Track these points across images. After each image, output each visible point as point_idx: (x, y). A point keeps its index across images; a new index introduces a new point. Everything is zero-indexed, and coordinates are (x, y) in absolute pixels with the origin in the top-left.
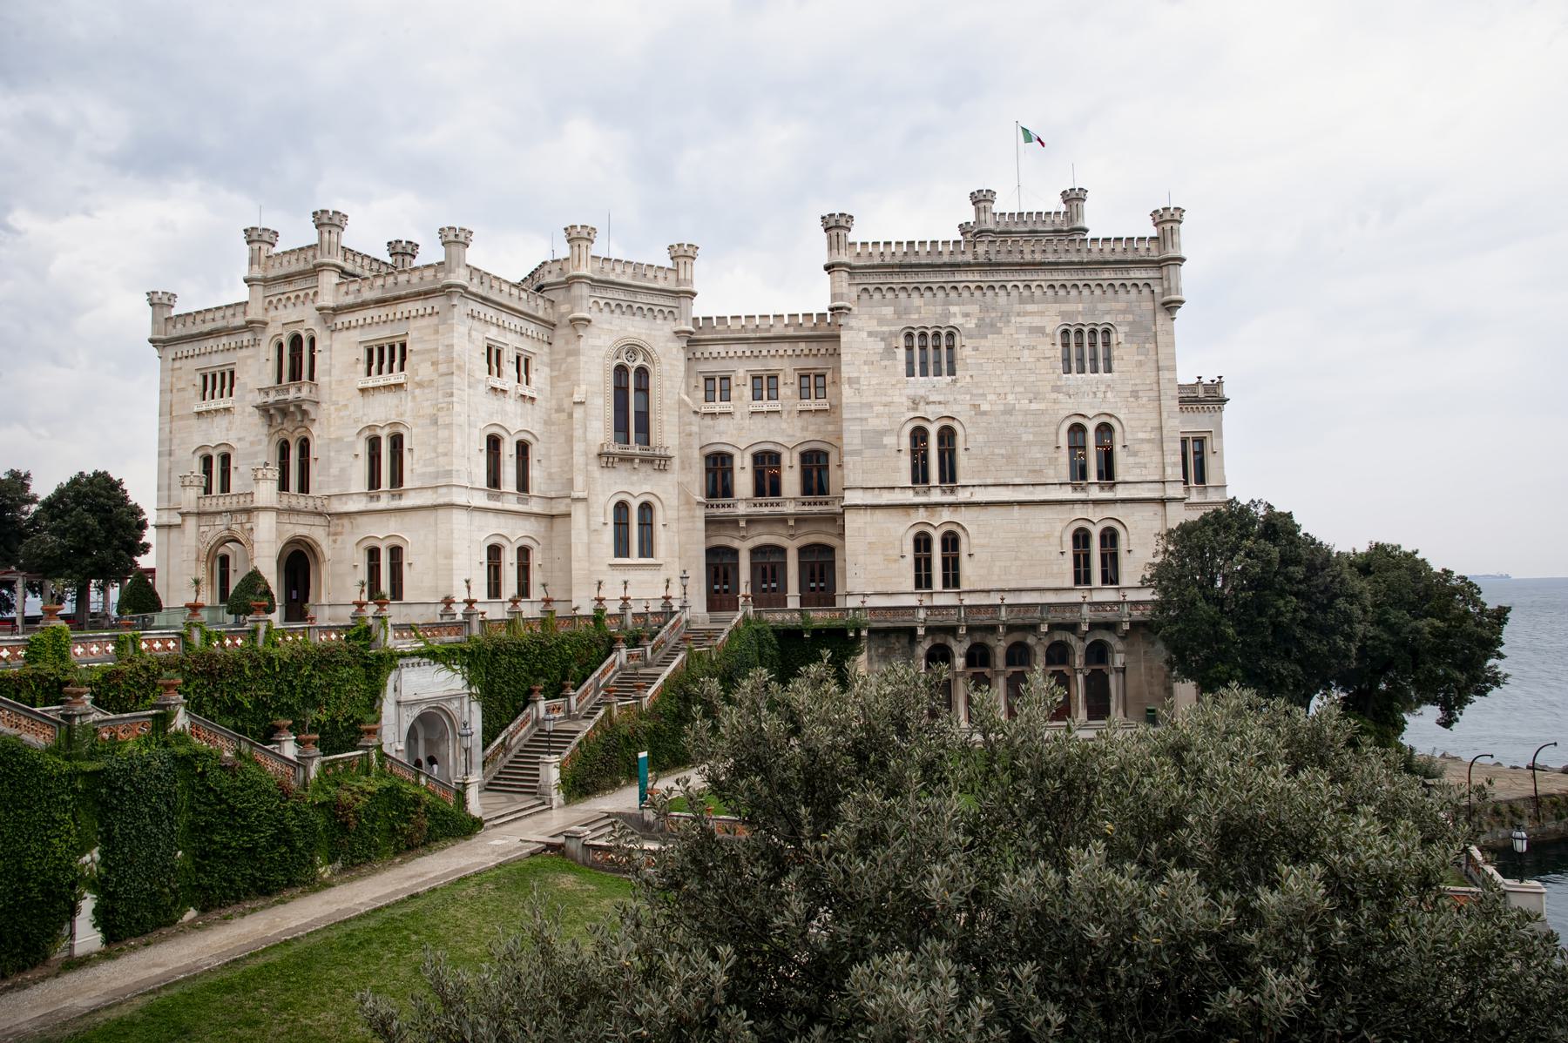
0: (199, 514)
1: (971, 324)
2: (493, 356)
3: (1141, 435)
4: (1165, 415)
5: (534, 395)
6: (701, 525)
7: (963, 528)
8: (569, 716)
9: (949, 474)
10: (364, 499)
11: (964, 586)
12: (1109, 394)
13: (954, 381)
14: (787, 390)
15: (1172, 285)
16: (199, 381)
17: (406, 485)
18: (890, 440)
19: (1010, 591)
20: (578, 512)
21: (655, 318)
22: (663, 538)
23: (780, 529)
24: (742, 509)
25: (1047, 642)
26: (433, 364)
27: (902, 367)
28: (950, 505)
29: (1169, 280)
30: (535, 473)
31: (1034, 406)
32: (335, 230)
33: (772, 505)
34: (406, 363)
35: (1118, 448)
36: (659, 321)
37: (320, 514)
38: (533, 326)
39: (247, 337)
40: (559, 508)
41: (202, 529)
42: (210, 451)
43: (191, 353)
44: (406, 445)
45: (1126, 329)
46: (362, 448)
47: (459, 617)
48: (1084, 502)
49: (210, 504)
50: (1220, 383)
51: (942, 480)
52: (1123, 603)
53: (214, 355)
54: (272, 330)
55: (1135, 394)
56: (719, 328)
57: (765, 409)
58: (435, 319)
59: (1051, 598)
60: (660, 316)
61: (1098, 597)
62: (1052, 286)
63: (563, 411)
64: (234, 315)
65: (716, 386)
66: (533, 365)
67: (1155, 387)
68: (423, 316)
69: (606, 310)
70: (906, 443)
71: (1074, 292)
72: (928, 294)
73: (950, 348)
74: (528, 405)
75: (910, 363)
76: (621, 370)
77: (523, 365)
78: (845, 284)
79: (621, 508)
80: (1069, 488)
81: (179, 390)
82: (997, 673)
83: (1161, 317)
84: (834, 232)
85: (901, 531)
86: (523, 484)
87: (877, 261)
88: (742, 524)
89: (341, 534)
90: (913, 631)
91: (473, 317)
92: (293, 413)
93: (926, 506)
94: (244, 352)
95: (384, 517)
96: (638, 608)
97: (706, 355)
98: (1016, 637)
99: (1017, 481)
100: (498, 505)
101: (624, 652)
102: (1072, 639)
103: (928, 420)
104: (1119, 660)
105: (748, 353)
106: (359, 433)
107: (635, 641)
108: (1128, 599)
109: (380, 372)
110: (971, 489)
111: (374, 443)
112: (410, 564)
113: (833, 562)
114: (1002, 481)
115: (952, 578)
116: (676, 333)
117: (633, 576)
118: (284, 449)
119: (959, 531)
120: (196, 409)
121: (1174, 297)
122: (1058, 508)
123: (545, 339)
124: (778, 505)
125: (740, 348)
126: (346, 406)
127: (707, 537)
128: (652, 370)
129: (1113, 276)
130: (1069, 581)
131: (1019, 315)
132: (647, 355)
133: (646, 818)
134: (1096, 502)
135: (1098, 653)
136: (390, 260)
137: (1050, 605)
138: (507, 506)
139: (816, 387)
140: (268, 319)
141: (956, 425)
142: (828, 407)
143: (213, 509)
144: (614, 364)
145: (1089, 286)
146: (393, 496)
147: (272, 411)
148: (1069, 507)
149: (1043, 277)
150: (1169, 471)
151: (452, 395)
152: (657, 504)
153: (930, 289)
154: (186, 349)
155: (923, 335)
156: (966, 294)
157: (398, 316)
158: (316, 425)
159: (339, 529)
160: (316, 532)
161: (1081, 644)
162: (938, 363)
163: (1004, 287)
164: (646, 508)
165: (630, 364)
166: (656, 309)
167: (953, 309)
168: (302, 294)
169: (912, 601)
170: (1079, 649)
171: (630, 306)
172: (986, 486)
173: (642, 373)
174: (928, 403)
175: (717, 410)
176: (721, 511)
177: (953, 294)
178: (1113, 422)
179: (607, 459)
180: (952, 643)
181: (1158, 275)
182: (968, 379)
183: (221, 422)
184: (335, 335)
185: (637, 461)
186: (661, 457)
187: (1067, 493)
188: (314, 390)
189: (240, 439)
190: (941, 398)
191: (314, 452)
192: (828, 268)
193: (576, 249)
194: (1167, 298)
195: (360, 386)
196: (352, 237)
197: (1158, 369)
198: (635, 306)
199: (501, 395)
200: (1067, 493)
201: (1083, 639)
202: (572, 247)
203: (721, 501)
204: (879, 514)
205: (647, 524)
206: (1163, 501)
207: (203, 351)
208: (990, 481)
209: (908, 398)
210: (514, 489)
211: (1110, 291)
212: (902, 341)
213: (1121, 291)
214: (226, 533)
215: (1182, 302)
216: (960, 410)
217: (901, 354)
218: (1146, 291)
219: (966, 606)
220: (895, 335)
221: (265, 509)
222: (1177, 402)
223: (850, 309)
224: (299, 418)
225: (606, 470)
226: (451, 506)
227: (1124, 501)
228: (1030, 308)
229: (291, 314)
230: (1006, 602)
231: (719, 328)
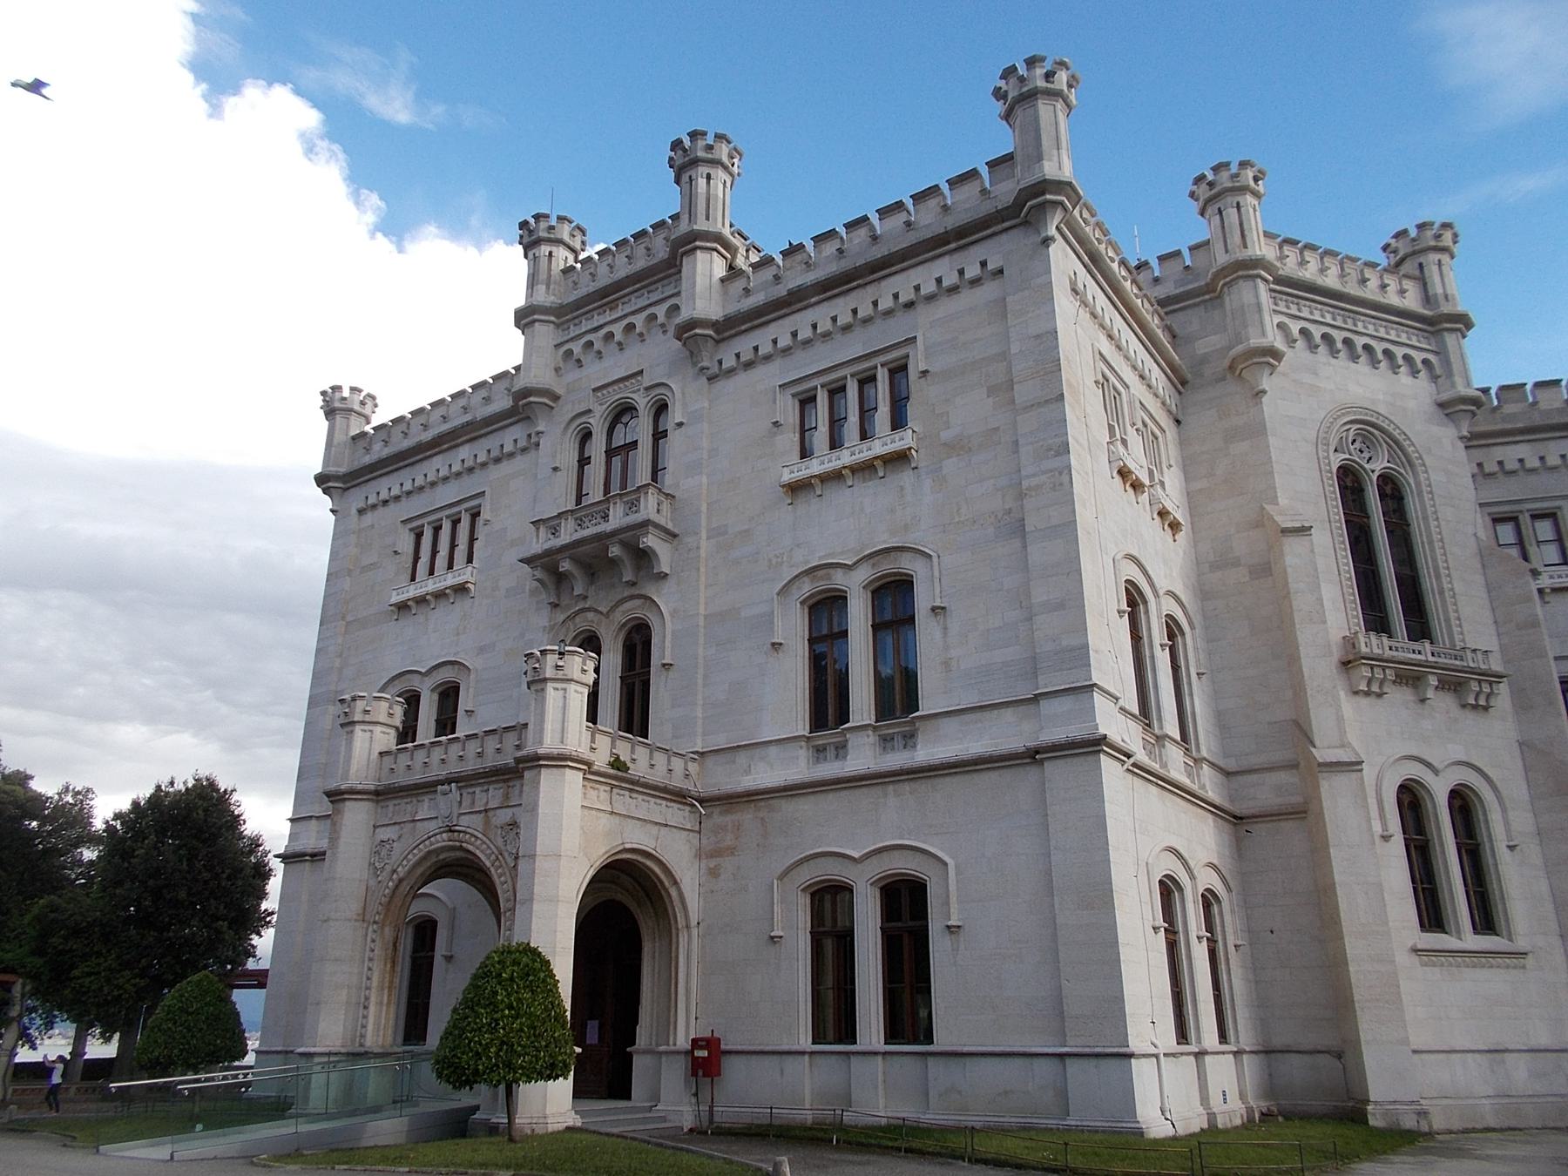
0: (381, 795)
10: (802, 754)
16: (406, 543)
17: (926, 706)
26: (992, 391)
32: (720, 175)
34: (912, 410)
37: (679, 796)
39: (512, 436)
41: (384, 834)
42: (415, 683)
43: (396, 491)
44: (923, 600)
46: (793, 628)
49: (414, 769)
53: (440, 489)
54: (566, 411)
58: (989, 290)
63: (1236, 563)
64: (487, 400)
68: (954, 290)
79: (1411, 800)
81: (365, 569)
89: (732, 851)
92: (614, 563)
94: (506, 468)
95: (863, 798)
97: (1491, 467)
106: (784, 590)
109: (835, 443)
116: (1442, 405)
120: (396, 598)
126: (746, 531)
128: (1409, 480)
132: (1396, 446)
140: (559, 391)
143: (417, 777)
144: (1336, 460)
147: (566, 566)
151: (1064, 449)
154: (387, 486)
158: (669, 587)
159: (729, 840)
166: (1399, 352)
168: (639, 320)
171: (1347, 342)
173: (1392, 490)
183: (444, 618)
184: (720, 385)
188: (665, 507)
189: (482, 650)
191: (663, 649)
193: (1231, 214)
195: (787, 477)
198: (1360, 341)
207: (419, 481)
214: (443, 840)
221: (561, 760)
224: (628, 576)
229: (613, 366)
231: (1510, 408)
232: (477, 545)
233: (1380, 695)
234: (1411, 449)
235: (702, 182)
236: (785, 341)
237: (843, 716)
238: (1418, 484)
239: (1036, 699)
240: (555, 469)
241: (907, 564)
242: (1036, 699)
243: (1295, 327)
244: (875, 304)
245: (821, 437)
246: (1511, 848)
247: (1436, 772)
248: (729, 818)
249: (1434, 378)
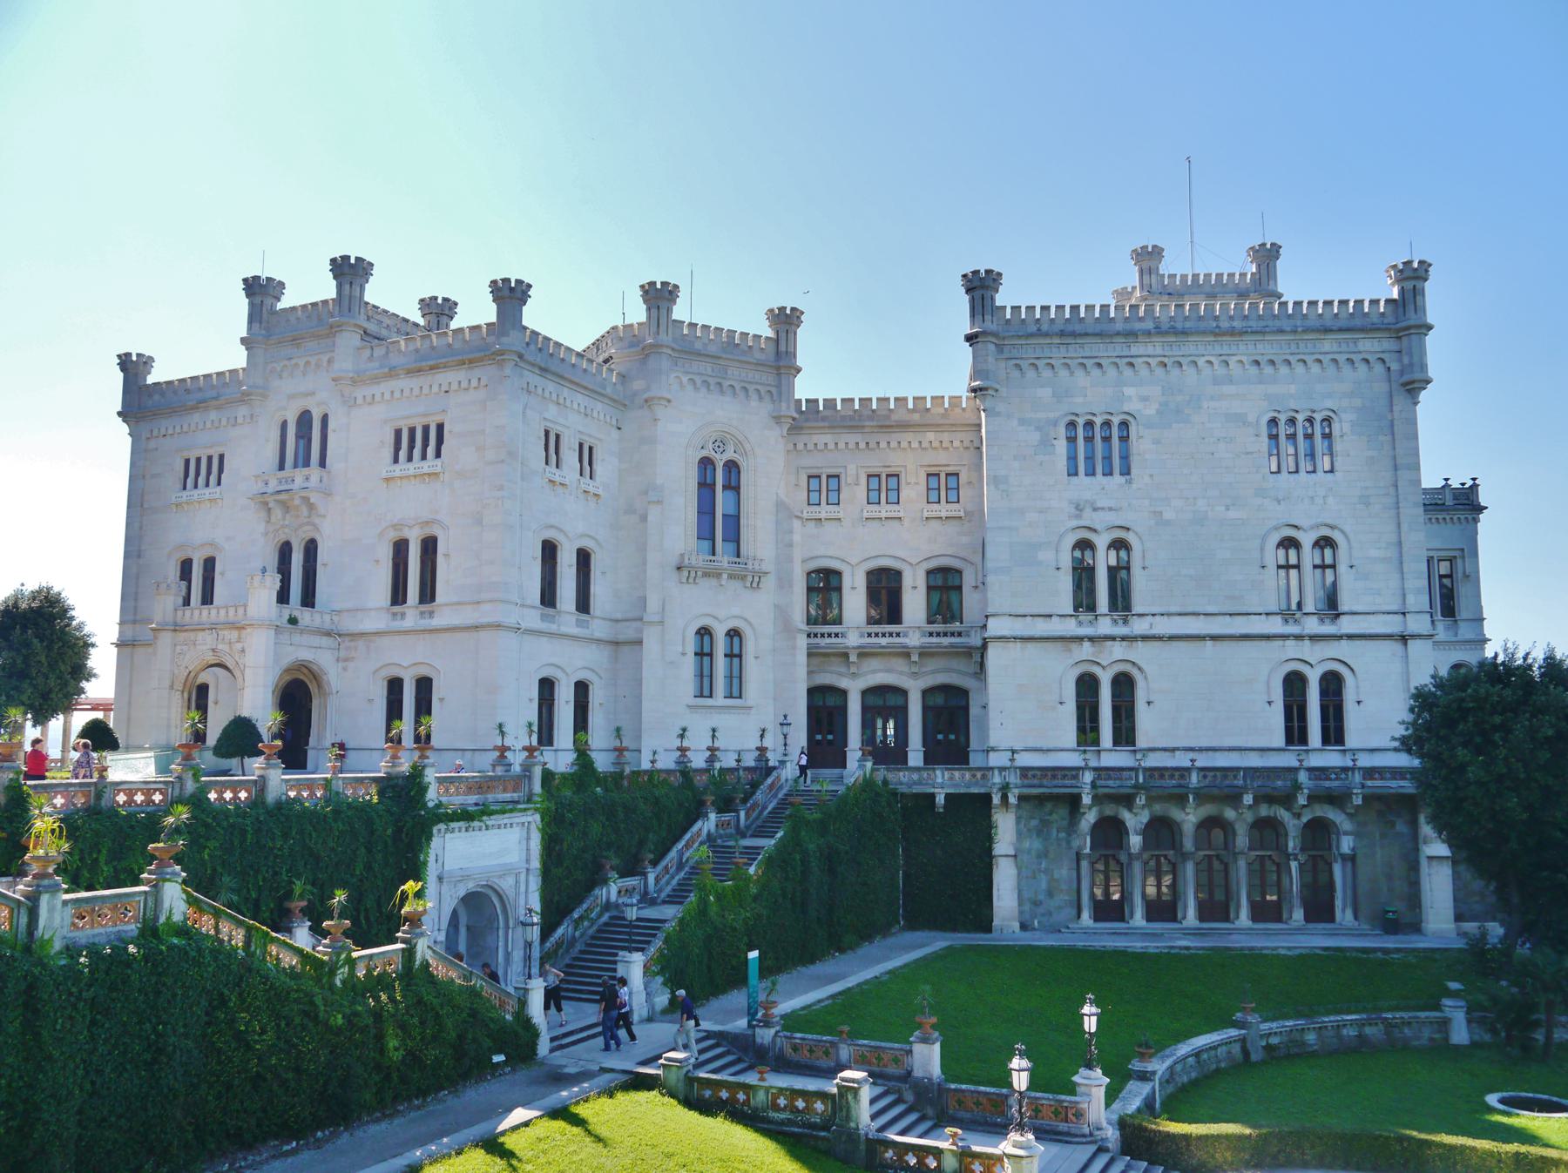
1: (1151, 410)
2: (552, 444)
3: (1374, 553)
4: (1404, 527)
5: (600, 492)
6: (802, 658)
7: (1140, 669)
8: (647, 900)
9: (1121, 600)
11: (1142, 741)
12: (1330, 500)
13: (1129, 482)
14: (913, 490)
15: (1416, 359)
18: (1046, 556)
19: (1201, 750)
20: (651, 638)
21: (747, 396)
22: (754, 671)
23: (899, 664)
24: (853, 640)
25: (1249, 817)
27: (1062, 463)
28: (1123, 638)
29: (1410, 354)
30: (598, 589)
31: (1232, 514)
33: (891, 635)
34: (444, 448)
35: (1342, 568)
36: (754, 403)
37: (328, 634)
38: (599, 406)
40: (628, 632)
42: (189, 554)
43: (170, 432)
45: (1353, 417)
46: (385, 555)
47: (517, 768)
48: (1299, 637)
50: (1474, 487)
51: (1113, 606)
52: (1353, 769)
55: (1365, 501)
56: (829, 413)
57: (884, 515)
59: (1255, 761)
60: (754, 396)
61: (1316, 761)
62: (1257, 363)
65: (823, 486)
67: (1392, 491)
69: (690, 388)
70: (1066, 561)
71: (1284, 370)
72: (1096, 372)
73: (1124, 439)
75: (1072, 458)
76: (706, 464)
77: (587, 455)
78: (990, 359)
79: (704, 633)
80: (1278, 619)
82: (1185, 856)
83: (1400, 401)
84: (978, 294)
85: (1060, 672)
86: (583, 604)
87: (1033, 328)
88: (853, 658)
90: (1074, 801)
91: (529, 392)
93: (1091, 639)
96: (728, 761)
98: (1208, 810)
99: (1210, 609)
100: (553, 628)
101: (713, 816)
102: (1283, 814)
103: (1095, 531)
104: (1346, 844)
105: (862, 445)
106: (381, 534)
107: (725, 805)
108: (1360, 764)
110: (1150, 618)
111: (400, 548)
112: (441, 700)
113: (966, 709)
114: (1190, 610)
115: (1125, 734)
117: (724, 721)
118: (285, 551)
119: (1135, 672)
121: (1417, 376)
122: (1263, 643)
123: (614, 422)
124: (898, 635)
125: (852, 438)
127: (810, 673)
128: (743, 464)
129: (1335, 348)
130: (1279, 740)
131: (1212, 398)
133: (759, 1040)
134: (1314, 638)
135: (1319, 832)
136: (421, 322)
137: (1255, 770)
138: (564, 629)
139: (947, 489)
141: (1131, 538)
142: (962, 514)
145: (1304, 362)
146: (422, 613)
148: (1279, 643)
149: (1244, 350)
150: (1411, 599)
153: (1099, 365)
155: (1089, 424)
156: (1144, 372)
157: (435, 389)
160: (321, 656)
161: (1296, 822)
162: (1108, 459)
163: (1195, 363)
164: (734, 634)
165: (718, 456)
166: (751, 388)
167: (1129, 391)
168: (313, 360)
169: (1073, 760)
170: (1293, 826)
172: (1169, 614)
173: (732, 467)
174: (1095, 509)
175: (823, 515)
176: (828, 640)
177: (1128, 372)
178: (1336, 535)
180: (1126, 816)
181: (1396, 348)
182: (1147, 479)
185: (725, 576)
186: (754, 573)
187: (1275, 626)
190: (1112, 503)
192: (970, 338)
194: (1406, 378)
195: (384, 475)
196: (376, 293)
197: (1396, 468)
198: (726, 383)
199: (560, 489)
200: (1275, 626)
201: (1298, 816)
202: (649, 309)
203: (826, 629)
204: (1030, 646)
205: (735, 656)
206: (1404, 639)
208: (1174, 609)
209: (1070, 502)
211: (1331, 369)
212: (1062, 431)
213: (1346, 369)
215: (1428, 381)
216: (1138, 520)
217: (1061, 446)
218: (1379, 369)
219: (1145, 770)
220: (1055, 423)
222: (1422, 509)
223: (997, 390)
225: (686, 587)
226: (498, 626)
227: (1351, 637)
228: (1228, 389)
230: (1198, 764)
231: (829, 413)
232: (223, 476)
233: (695, 583)
234: (747, 446)
235: (347, 287)
236: (387, 396)
237: (404, 601)
238: (748, 465)
239: (478, 603)
240: (267, 441)
241: (436, 531)
242: (478, 603)
243: (685, 379)
244: (431, 386)
245: (403, 454)
246: (756, 658)
247: (721, 622)
248: (352, 644)
249: (773, 401)
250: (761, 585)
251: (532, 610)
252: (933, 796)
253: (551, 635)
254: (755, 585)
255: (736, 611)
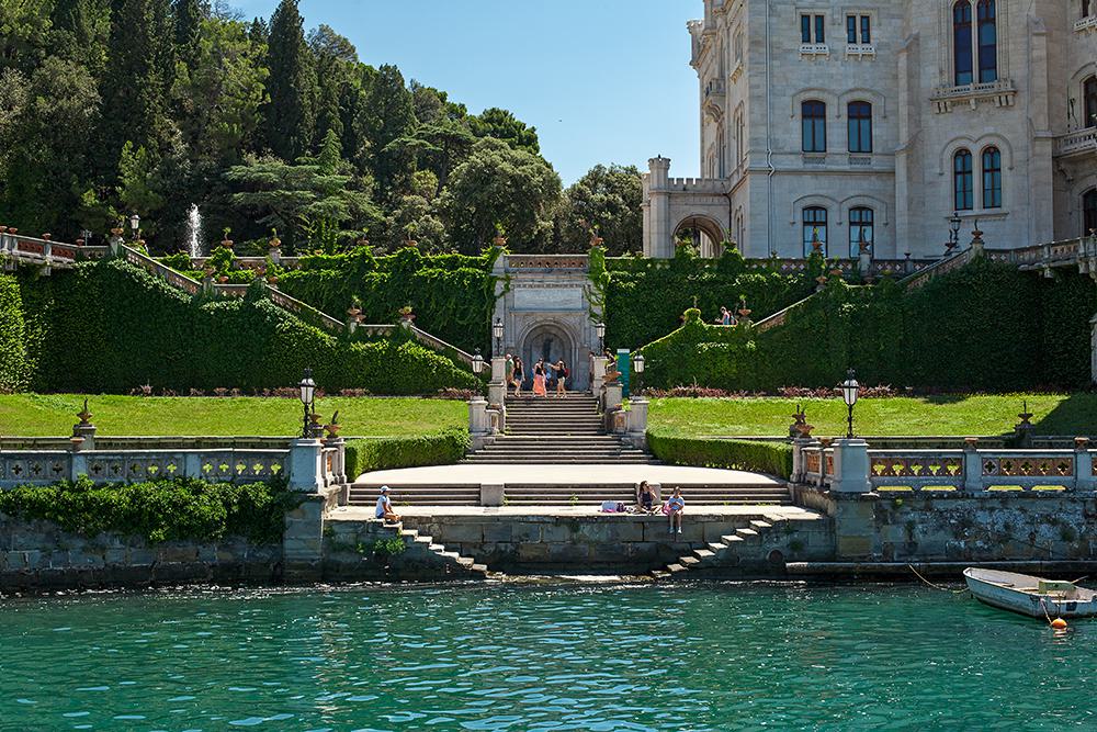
5: (873, 52)
22: (1008, 179)
66: (874, 22)
74: (867, 64)
79: (962, 154)
86: (860, 144)
138: (830, 167)
152: (1002, 147)
164: (991, 152)
179: (941, 104)
185: (972, 101)
199: (823, 59)
205: (992, 169)
210: (845, 150)
225: (941, 116)
246: (1011, 169)
250: (1011, 103)
251: (793, 157)
252: (1043, 270)
253: (815, 173)
254: (1004, 104)
255: (991, 130)
